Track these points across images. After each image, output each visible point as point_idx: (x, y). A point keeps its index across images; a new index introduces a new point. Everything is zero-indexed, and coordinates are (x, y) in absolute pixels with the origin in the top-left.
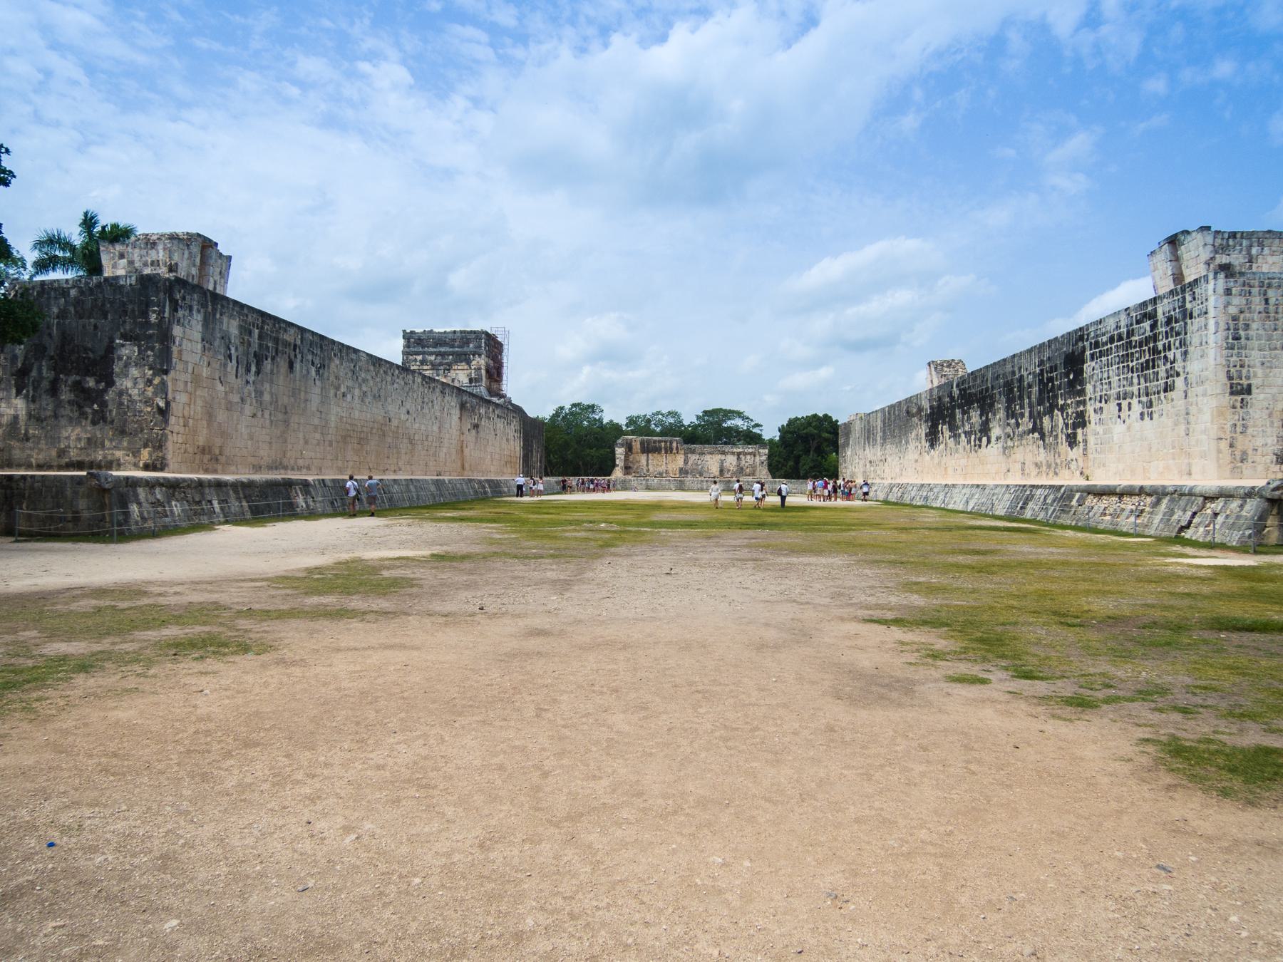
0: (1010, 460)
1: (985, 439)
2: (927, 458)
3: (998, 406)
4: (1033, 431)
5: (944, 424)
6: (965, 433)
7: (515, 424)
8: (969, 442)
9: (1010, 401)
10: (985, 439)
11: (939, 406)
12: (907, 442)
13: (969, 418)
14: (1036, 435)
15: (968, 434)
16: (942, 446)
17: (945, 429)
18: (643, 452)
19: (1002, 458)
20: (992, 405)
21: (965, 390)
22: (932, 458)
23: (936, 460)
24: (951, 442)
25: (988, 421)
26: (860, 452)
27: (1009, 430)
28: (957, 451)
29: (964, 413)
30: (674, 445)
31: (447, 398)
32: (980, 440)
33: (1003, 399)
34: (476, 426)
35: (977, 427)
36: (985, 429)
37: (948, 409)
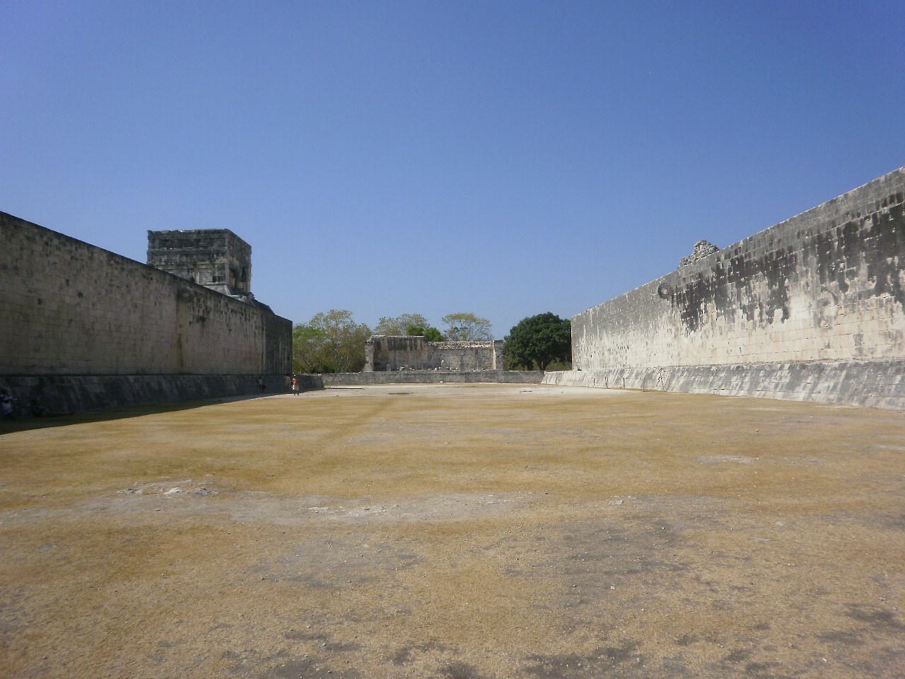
0: (830, 333)
1: (779, 313)
2: (685, 340)
3: (800, 268)
4: (880, 289)
5: (708, 300)
6: (744, 308)
7: (255, 320)
8: (750, 317)
9: (824, 260)
10: (779, 313)
11: (699, 284)
12: (656, 327)
13: (749, 291)
14: (886, 296)
15: (748, 310)
16: (707, 326)
17: (709, 308)
18: (390, 349)
19: (815, 332)
20: (789, 270)
21: (740, 260)
22: (692, 340)
23: (698, 342)
24: (722, 321)
25: (783, 290)
26: (596, 342)
27: (824, 295)
28: (730, 329)
29: (739, 285)
30: (419, 342)
31: (154, 285)
32: (771, 313)
33: (813, 259)
34: (202, 319)
35: (765, 299)
36: (780, 299)
37: (713, 285)
